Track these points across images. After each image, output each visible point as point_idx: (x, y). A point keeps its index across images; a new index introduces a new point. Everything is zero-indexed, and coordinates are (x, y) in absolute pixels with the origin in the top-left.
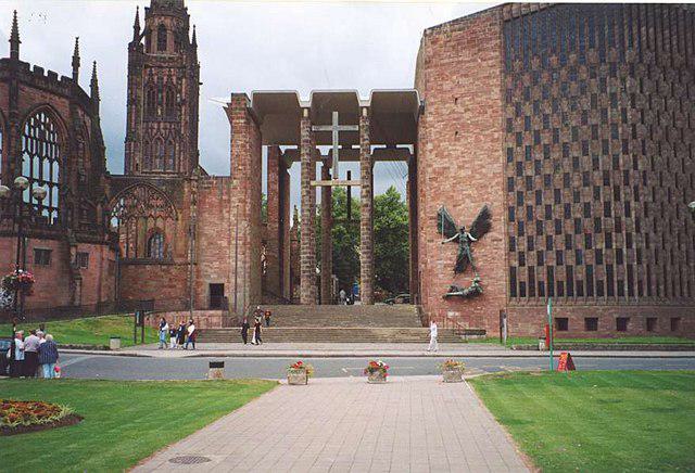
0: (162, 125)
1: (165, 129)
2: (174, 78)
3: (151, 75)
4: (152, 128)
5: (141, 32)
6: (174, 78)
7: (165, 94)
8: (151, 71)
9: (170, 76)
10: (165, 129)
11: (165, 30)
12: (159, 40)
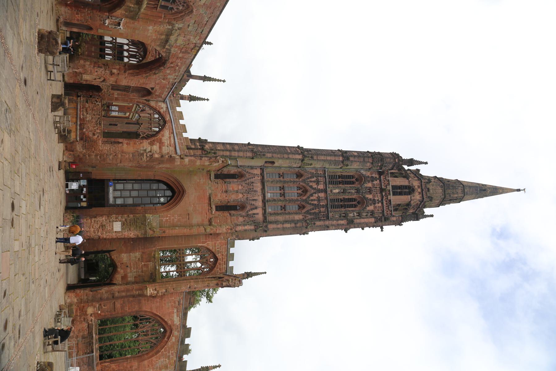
0: (322, 195)
1: (319, 199)
2: (371, 208)
3: (373, 179)
4: (318, 182)
5: (406, 167)
6: (371, 208)
7: (354, 197)
8: (376, 179)
9: (374, 202)
10: (319, 199)
11: (409, 193)
12: (400, 187)
